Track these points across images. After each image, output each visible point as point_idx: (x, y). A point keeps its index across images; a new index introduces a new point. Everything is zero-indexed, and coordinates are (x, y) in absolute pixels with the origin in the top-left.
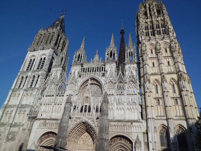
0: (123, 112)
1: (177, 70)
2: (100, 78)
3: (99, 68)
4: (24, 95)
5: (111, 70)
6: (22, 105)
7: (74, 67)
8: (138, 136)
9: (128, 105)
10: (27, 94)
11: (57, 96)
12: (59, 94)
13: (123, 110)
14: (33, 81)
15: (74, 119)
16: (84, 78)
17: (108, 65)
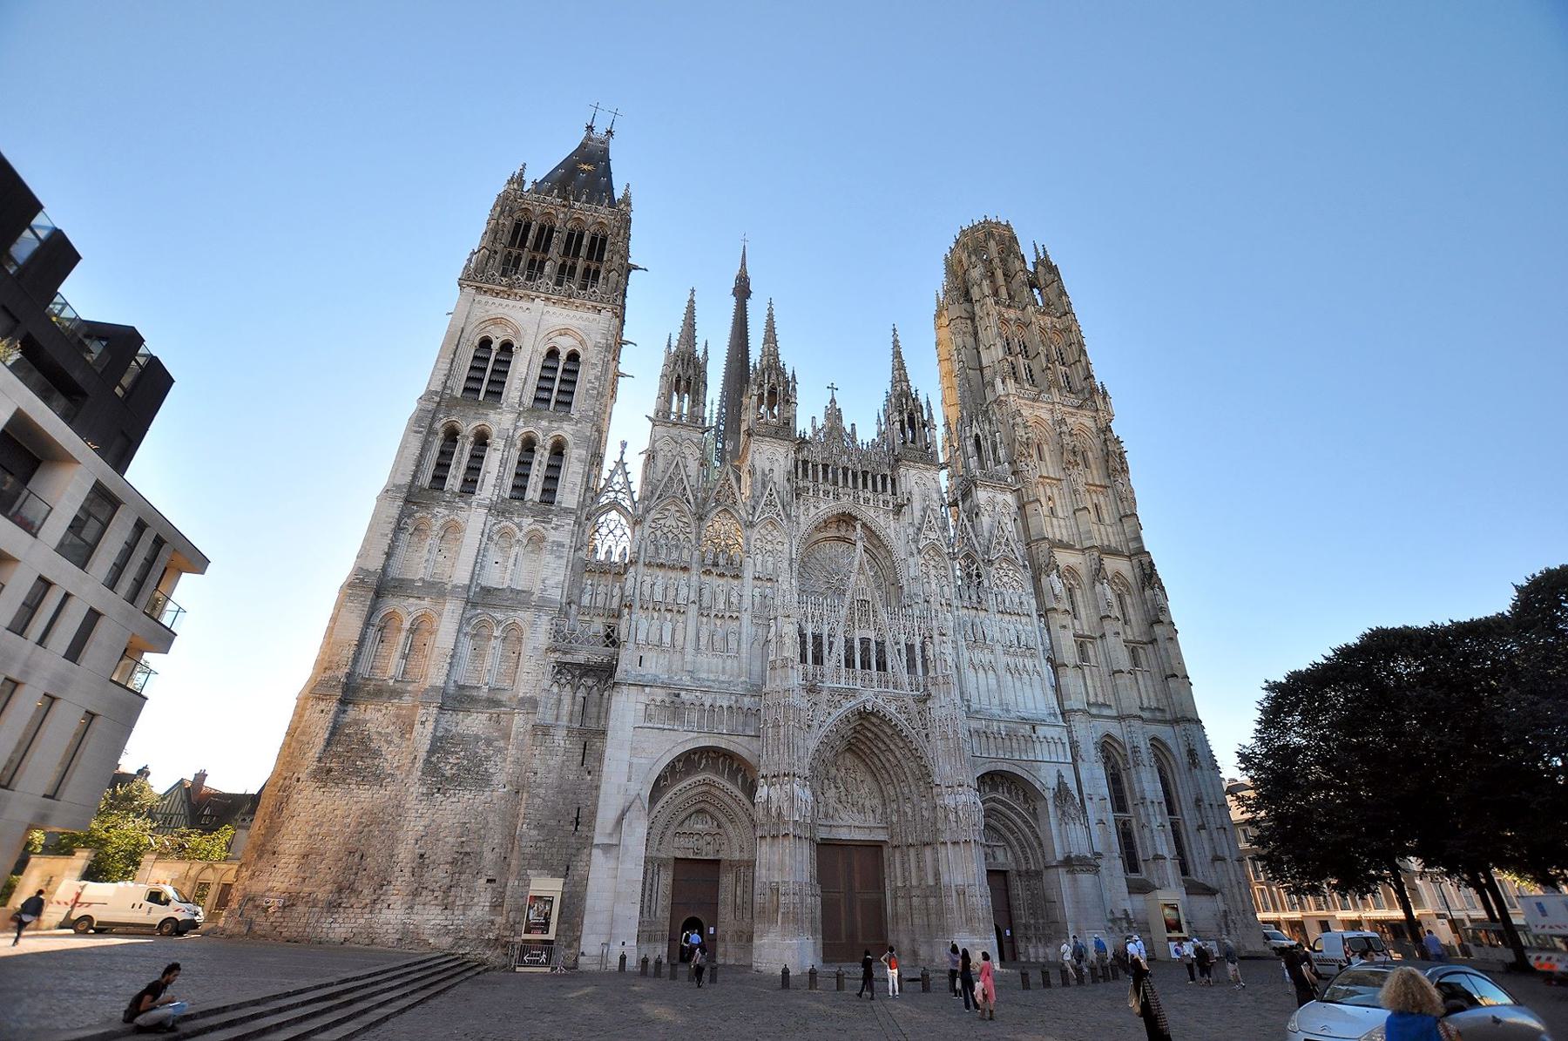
0: (995, 681)
1: (1132, 545)
2: (881, 521)
3: (869, 477)
4: (489, 538)
5: (925, 497)
6: (487, 591)
7: (765, 448)
8: (1060, 776)
9: (1006, 653)
10: (505, 534)
11: (708, 572)
12: (716, 564)
13: (991, 672)
14: (524, 465)
15: (825, 695)
16: (812, 511)
17: (913, 472)
